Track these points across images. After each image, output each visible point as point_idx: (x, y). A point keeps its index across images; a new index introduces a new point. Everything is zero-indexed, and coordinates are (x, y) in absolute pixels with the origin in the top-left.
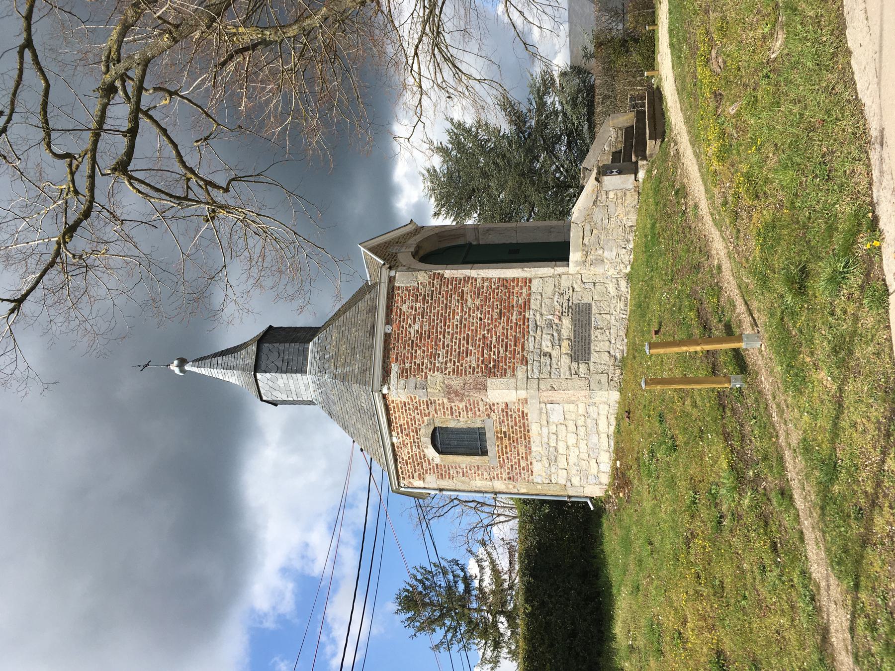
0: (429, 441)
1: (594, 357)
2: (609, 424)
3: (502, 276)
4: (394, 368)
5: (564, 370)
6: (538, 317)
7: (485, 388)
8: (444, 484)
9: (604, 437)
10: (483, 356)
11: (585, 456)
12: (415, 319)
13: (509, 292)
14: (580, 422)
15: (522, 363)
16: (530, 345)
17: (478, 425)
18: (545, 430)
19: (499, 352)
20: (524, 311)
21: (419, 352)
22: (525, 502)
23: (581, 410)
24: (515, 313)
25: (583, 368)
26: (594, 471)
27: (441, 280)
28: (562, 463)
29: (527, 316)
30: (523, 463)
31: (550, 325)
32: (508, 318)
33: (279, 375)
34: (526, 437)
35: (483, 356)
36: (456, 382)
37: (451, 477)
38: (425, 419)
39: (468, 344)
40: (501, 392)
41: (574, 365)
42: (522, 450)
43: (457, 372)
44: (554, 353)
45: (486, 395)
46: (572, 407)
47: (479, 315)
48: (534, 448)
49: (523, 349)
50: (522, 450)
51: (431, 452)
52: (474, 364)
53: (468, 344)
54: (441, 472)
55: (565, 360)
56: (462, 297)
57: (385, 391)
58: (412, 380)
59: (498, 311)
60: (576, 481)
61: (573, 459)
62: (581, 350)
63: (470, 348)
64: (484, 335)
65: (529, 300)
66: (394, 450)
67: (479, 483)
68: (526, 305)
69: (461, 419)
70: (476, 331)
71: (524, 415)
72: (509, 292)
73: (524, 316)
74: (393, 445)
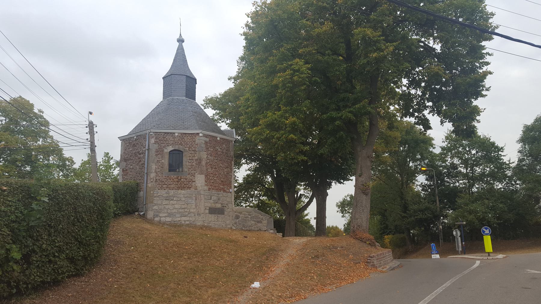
0: (177, 148)
1: (210, 215)
2: (185, 221)
4: (208, 140)
5: (207, 204)
7: (202, 174)
8: (153, 152)
9: (179, 219)
11: (169, 211)
14: (186, 210)
16: (214, 192)
17: (186, 170)
18: (182, 196)
22: (138, 185)
23: (192, 210)
25: (207, 211)
26: (161, 215)
28: (167, 202)
30: (164, 186)
31: (219, 199)
33: (185, 85)
34: (178, 188)
36: (204, 163)
37: (156, 155)
38: (187, 149)
40: (200, 180)
41: (208, 208)
42: (172, 186)
43: (207, 164)
44: (211, 201)
45: (199, 174)
46: (194, 207)
48: (172, 191)
50: (172, 186)
51: (170, 148)
52: (209, 170)
54: (159, 152)
55: (209, 205)
57: (201, 135)
58: (203, 146)
60: (155, 207)
61: (167, 207)
62: (213, 211)
66: (171, 133)
67: (154, 167)
68: (224, 191)
69: (187, 163)
71: (190, 188)
74: (174, 133)
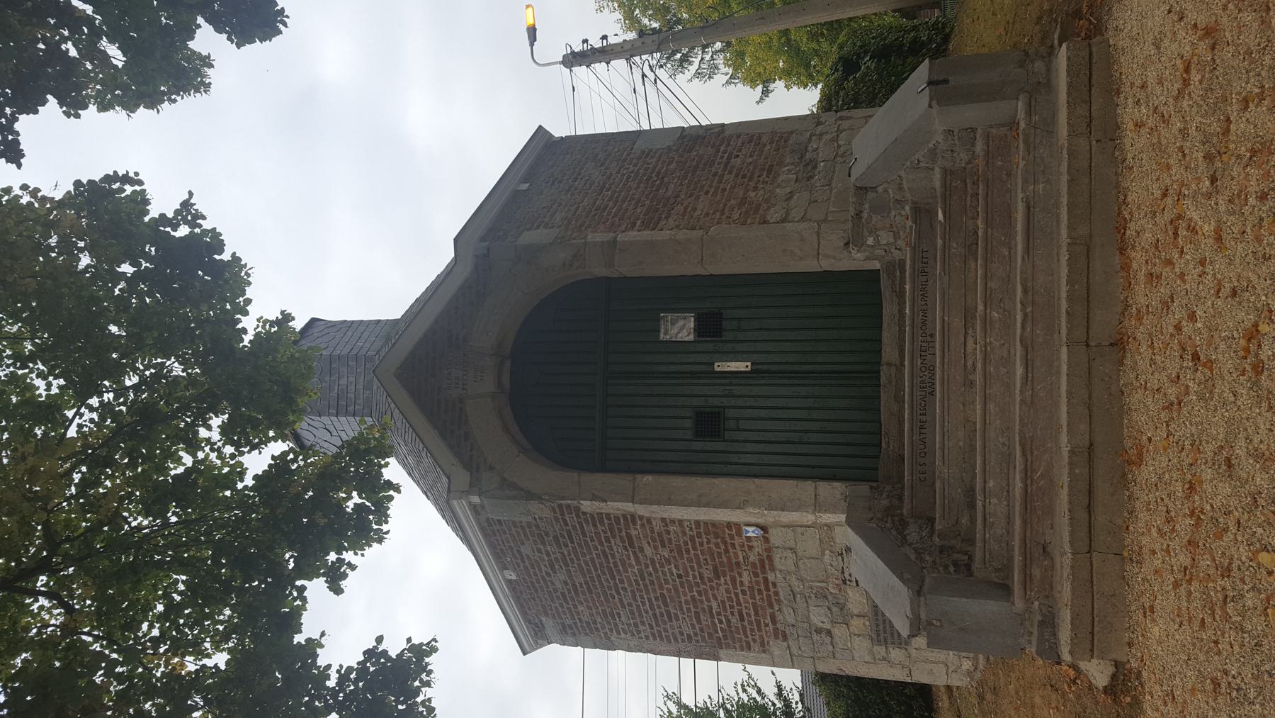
3: (702, 518)
6: (795, 582)
10: (699, 622)
12: (552, 567)
13: (725, 543)
15: (777, 638)
19: (728, 621)
20: (764, 572)
21: (581, 608)
24: (745, 574)
27: (578, 517)
29: (771, 577)
32: (733, 580)
35: (699, 622)
39: (666, 605)
44: (836, 631)
47: (674, 571)
49: (774, 621)
53: (666, 605)
56: (631, 544)
59: (710, 567)
63: (672, 611)
64: (693, 597)
65: (770, 558)
68: (766, 562)
70: (676, 590)
72: (725, 543)
73: (766, 580)
